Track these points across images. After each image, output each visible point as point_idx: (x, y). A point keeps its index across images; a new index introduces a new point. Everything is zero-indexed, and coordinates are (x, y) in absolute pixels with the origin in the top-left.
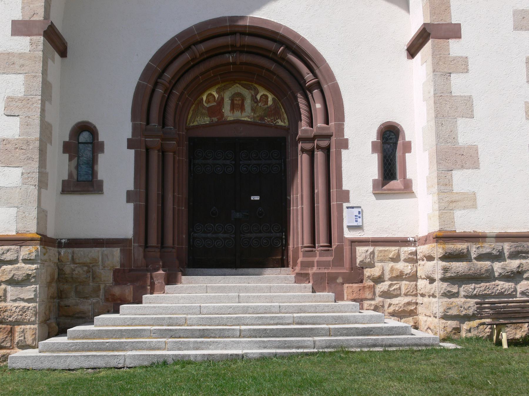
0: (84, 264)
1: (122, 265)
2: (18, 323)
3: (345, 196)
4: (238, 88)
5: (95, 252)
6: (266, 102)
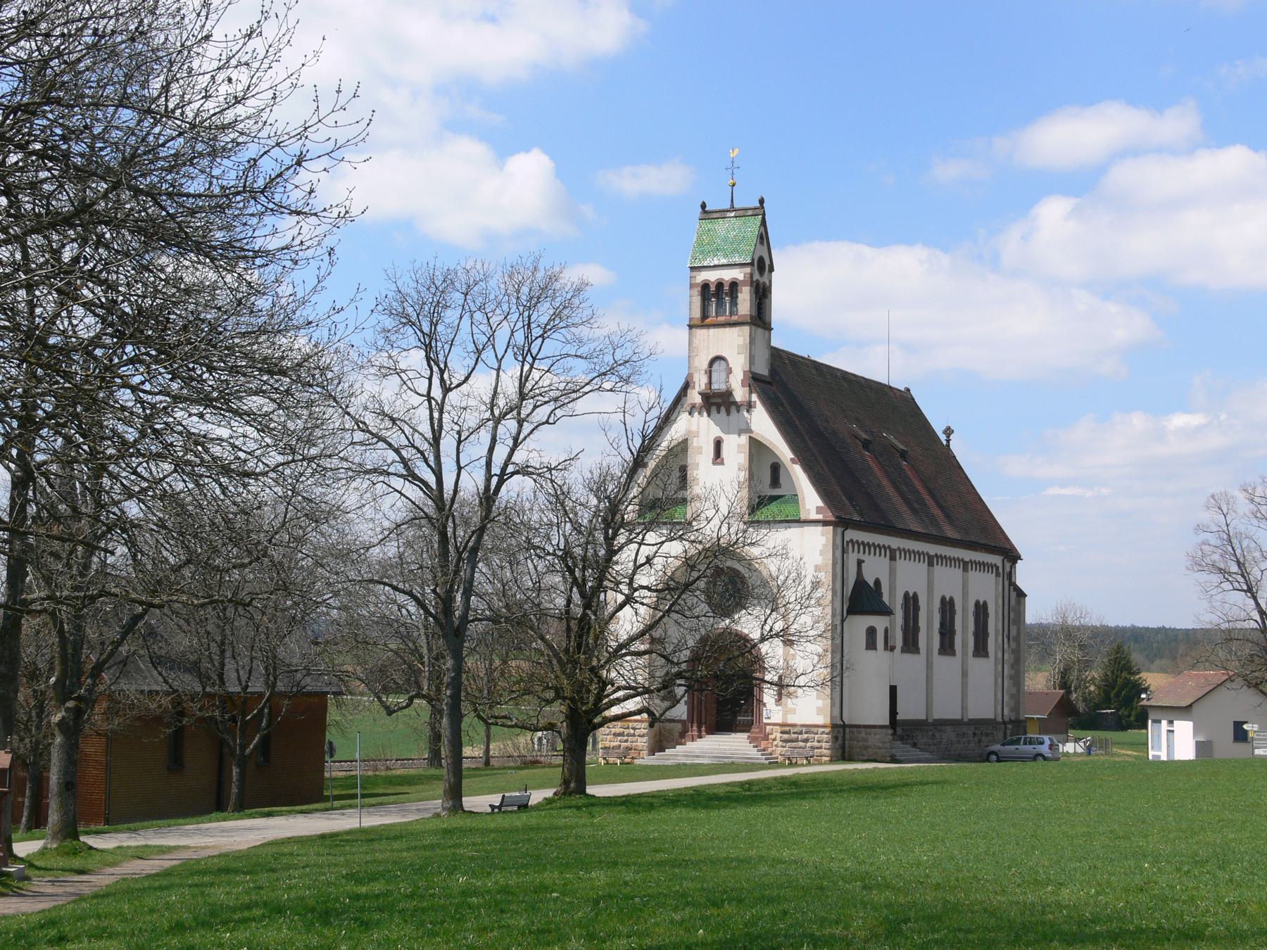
5: (672, 725)
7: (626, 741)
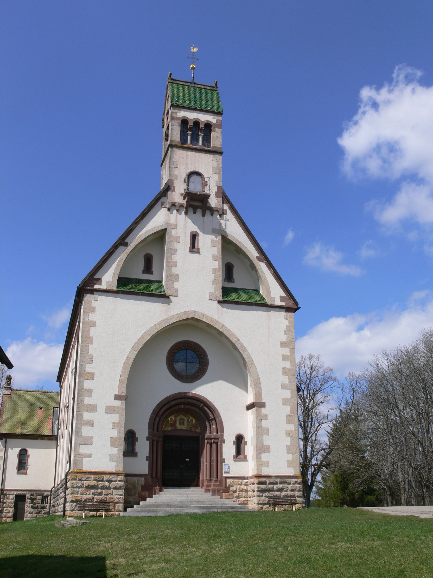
0: (131, 483)
1: (144, 484)
2: (117, 503)
3: (223, 461)
4: (182, 416)
5: (135, 479)
6: (192, 422)
7: (100, 494)
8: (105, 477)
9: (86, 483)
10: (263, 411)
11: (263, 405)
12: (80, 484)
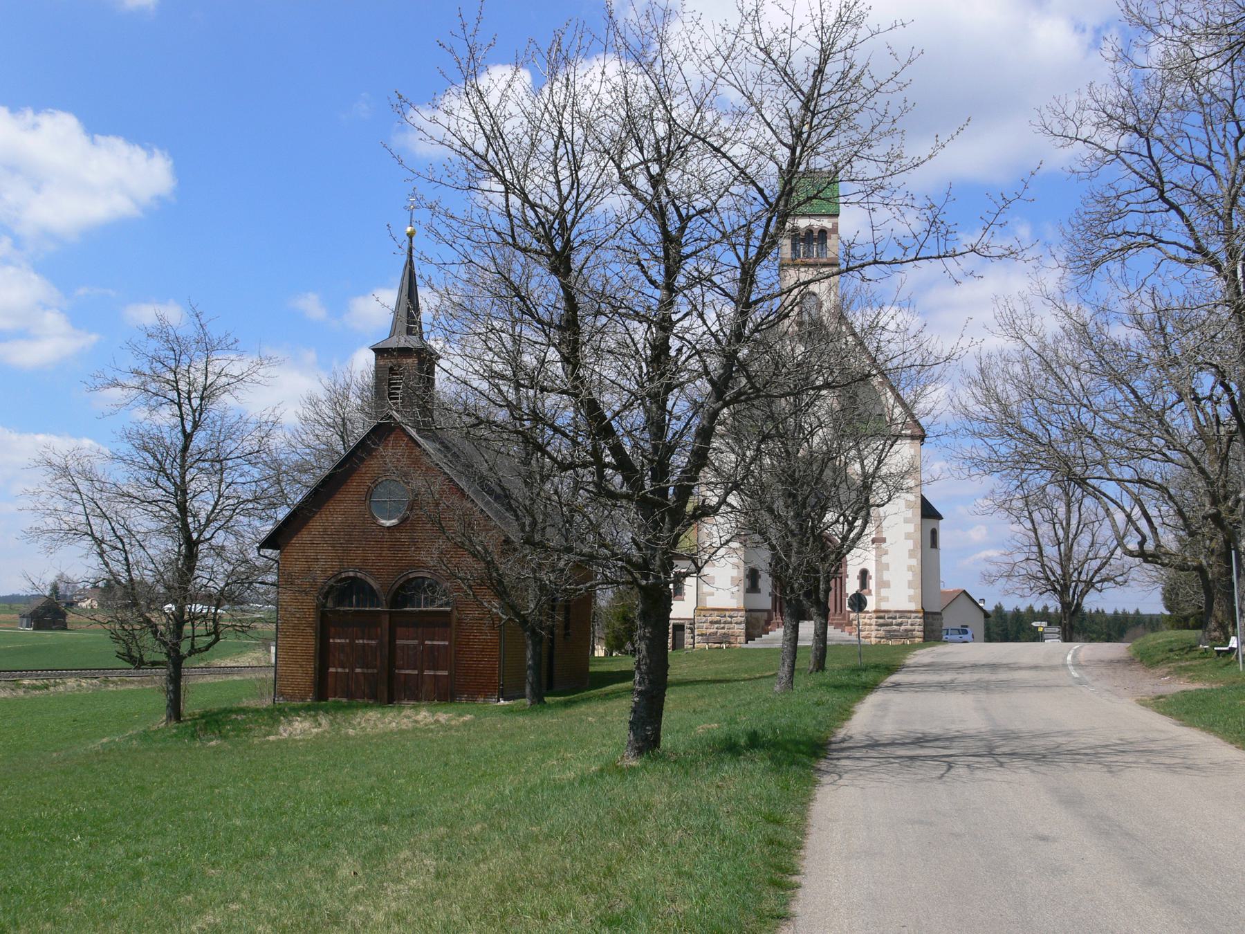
7: (723, 628)
8: (727, 613)
9: (710, 619)
10: (883, 545)
11: (884, 540)
12: (704, 619)
